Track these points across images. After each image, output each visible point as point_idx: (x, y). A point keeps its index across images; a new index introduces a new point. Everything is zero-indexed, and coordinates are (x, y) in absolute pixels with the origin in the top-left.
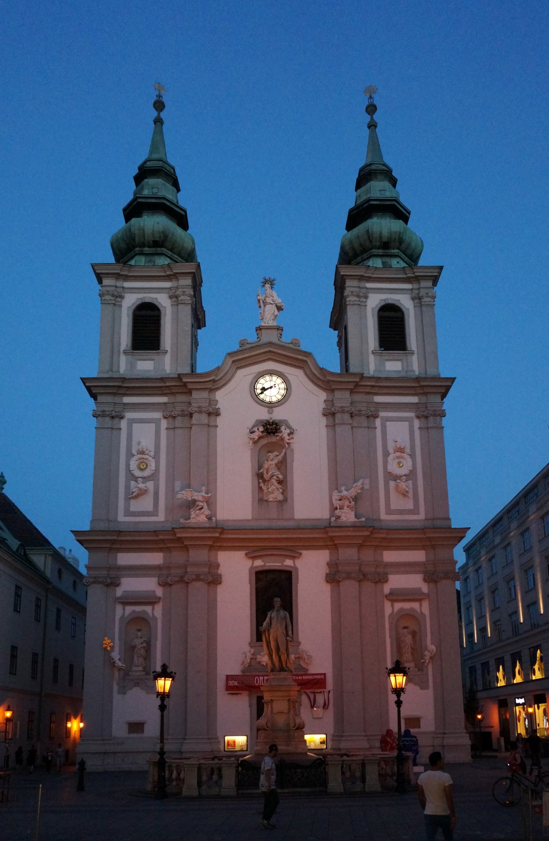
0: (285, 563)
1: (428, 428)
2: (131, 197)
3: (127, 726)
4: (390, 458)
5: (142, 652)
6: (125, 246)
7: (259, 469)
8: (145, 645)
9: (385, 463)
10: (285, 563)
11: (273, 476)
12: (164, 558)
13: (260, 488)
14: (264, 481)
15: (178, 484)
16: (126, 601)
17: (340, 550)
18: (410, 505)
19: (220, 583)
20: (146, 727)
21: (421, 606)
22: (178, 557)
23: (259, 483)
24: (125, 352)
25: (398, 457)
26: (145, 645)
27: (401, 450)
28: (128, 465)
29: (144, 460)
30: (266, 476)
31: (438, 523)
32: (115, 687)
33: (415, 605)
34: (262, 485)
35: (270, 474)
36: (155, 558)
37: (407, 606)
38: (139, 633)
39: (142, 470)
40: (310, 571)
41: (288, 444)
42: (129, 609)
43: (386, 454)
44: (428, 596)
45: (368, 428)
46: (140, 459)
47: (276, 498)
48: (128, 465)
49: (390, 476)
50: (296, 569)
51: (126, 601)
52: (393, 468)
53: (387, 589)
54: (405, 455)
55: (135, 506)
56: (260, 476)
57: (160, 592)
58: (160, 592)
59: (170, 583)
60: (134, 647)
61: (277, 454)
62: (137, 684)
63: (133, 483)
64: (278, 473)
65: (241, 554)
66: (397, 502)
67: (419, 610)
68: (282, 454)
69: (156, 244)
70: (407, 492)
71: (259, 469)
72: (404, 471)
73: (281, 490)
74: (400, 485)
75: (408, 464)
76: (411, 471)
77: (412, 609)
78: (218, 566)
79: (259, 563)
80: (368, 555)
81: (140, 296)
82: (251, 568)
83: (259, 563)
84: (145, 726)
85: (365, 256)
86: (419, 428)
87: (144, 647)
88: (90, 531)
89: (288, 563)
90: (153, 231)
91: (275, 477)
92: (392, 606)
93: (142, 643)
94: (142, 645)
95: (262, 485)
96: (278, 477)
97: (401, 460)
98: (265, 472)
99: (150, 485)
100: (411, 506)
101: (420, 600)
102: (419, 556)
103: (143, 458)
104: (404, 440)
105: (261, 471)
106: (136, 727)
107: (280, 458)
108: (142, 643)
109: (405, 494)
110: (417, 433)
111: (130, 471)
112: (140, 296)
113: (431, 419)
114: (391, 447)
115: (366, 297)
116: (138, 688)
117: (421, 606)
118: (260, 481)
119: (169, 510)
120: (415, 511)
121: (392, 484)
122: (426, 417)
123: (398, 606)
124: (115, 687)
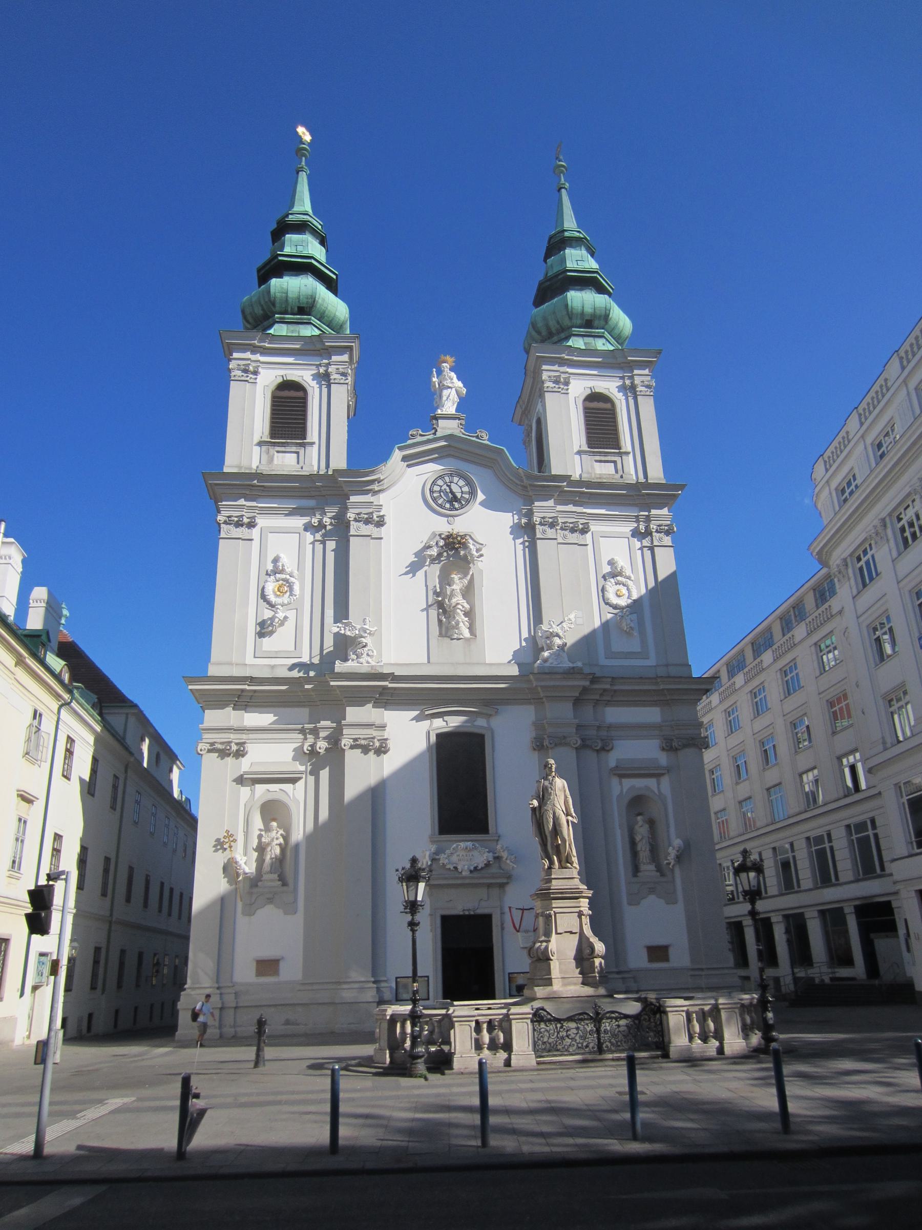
2: (268, 256)
3: (255, 964)
6: (261, 312)
10: (476, 723)
18: (636, 647)
21: (659, 784)
24: (260, 444)
31: (673, 671)
32: (240, 905)
33: (651, 783)
37: (640, 783)
44: (668, 770)
53: (613, 759)
62: (270, 901)
69: (302, 310)
77: (647, 788)
81: (282, 372)
84: (282, 964)
85: (563, 335)
90: (299, 298)
92: (621, 784)
100: (637, 649)
101: (658, 776)
102: (651, 715)
106: (268, 966)
112: (282, 372)
115: (567, 383)
116: (272, 906)
117: (659, 784)
120: (643, 655)
123: (628, 783)
124: (240, 905)
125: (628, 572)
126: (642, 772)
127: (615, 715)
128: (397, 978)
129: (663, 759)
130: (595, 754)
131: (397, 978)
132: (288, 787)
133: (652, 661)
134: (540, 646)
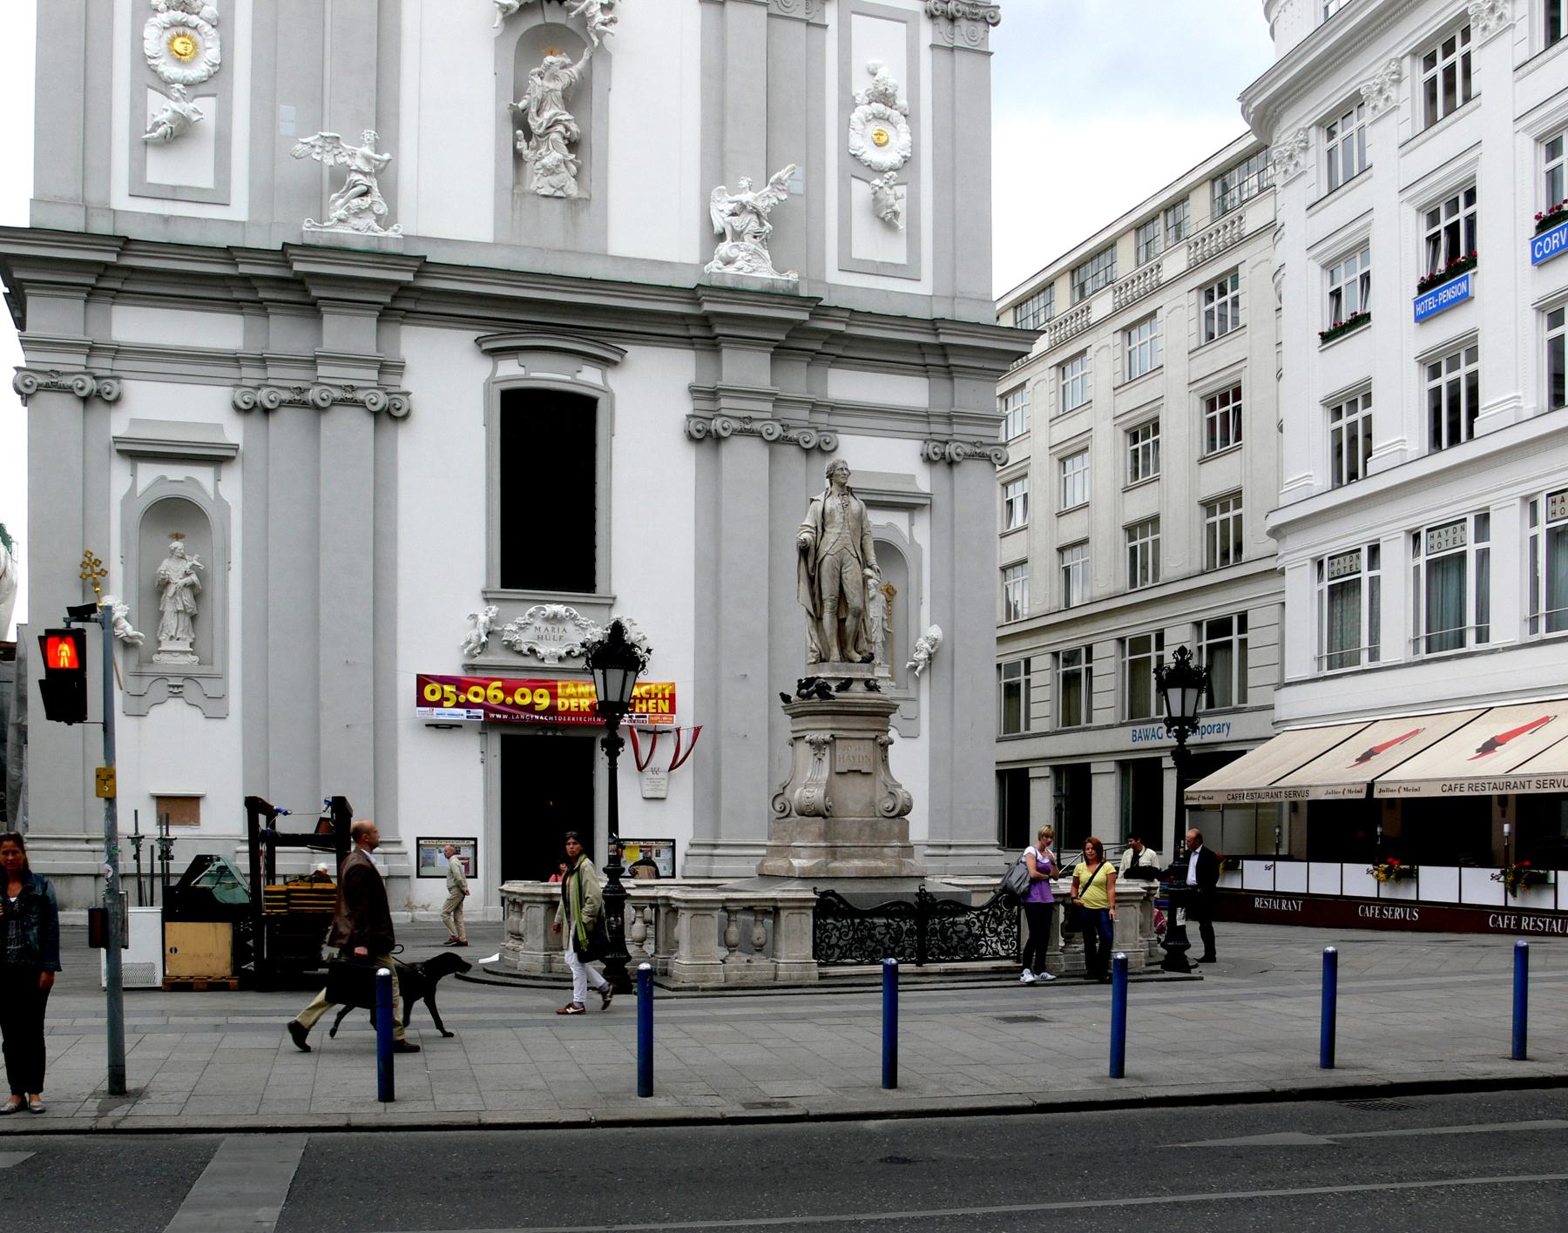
0: (580, 377)
1: (952, 49)
3: (154, 803)
4: (858, 115)
5: (187, 597)
7: (517, 99)
8: (194, 578)
9: (845, 126)
11: (557, 122)
12: (248, 331)
13: (518, 156)
14: (529, 135)
15: (287, 111)
16: (137, 454)
17: (727, 354)
18: (894, 251)
19: (406, 417)
20: (204, 809)
21: (912, 524)
22: (284, 334)
23: (516, 139)
25: (877, 117)
26: (194, 578)
27: (885, 98)
28: (138, 39)
29: (188, 31)
30: (536, 123)
34: (522, 145)
35: (547, 115)
36: (221, 331)
38: (177, 544)
39: (179, 58)
40: (644, 408)
41: (600, 35)
42: (149, 473)
43: (848, 104)
45: (808, 24)
46: (173, 25)
47: (561, 188)
48: (138, 39)
49: (857, 167)
50: (612, 397)
51: (137, 454)
52: (861, 143)
54: (894, 114)
55: (161, 169)
56: (520, 121)
57: (234, 432)
58: (234, 432)
59: (269, 405)
60: (165, 584)
61: (568, 61)
62: (176, 692)
63: (153, 95)
64: (567, 116)
65: (462, 340)
66: (869, 243)
67: (906, 531)
68: (580, 65)
70: (896, 214)
71: (517, 99)
72: (888, 157)
73: (573, 168)
74: (881, 195)
75: (899, 141)
76: (906, 160)
78: (399, 368)
79: (512, 371)
80: (796, 380)
82: (489, 384)
83: (512, 371)
84: (203, 805)
86: (933, 46)
87: (192, 586)
88: (31, 230)
89: (588, 378)
91: (560, 128)
93: (187, 574)
94: (187, 580)
95: (522, 145)
96: (567, 129)
97: (884, 127)
98: (533, 110)
99: (204, 109)
100: (901, 258)
102: (910, 391)
103: (184, 24)
104: (893, 76)
105: (522, 105)
107: (574, 70)
108: (187, 574)
109: (889, 224)
110: (926, 57)
111: (145, 57)
113: (963, 25)
114: (861, 87)
117: (912, 524)
118: (520, 132)
119: (263, 192)
120: (908, 272)
121: (861, 192)
122: (952, 19)
125: (902, 101)
126: (885, 499)
127: (845, 385)
128: (418, 839)
129: (924, 480)
130: (802, 457)
131: (418, 839)
132: (203, 475)
133: (925, 287)
134: (718, 229)
